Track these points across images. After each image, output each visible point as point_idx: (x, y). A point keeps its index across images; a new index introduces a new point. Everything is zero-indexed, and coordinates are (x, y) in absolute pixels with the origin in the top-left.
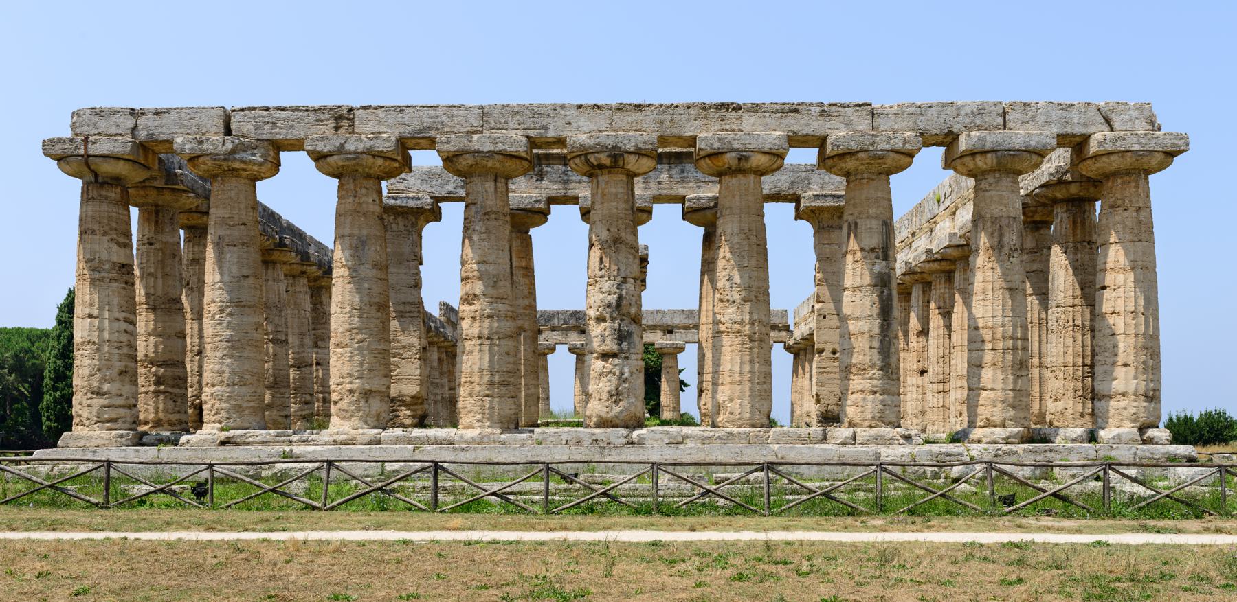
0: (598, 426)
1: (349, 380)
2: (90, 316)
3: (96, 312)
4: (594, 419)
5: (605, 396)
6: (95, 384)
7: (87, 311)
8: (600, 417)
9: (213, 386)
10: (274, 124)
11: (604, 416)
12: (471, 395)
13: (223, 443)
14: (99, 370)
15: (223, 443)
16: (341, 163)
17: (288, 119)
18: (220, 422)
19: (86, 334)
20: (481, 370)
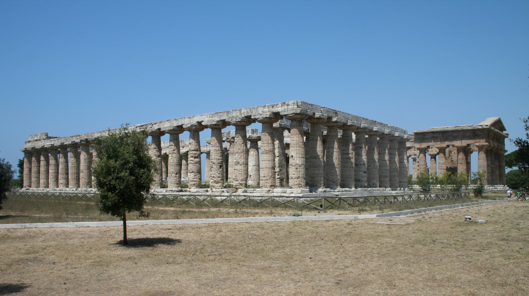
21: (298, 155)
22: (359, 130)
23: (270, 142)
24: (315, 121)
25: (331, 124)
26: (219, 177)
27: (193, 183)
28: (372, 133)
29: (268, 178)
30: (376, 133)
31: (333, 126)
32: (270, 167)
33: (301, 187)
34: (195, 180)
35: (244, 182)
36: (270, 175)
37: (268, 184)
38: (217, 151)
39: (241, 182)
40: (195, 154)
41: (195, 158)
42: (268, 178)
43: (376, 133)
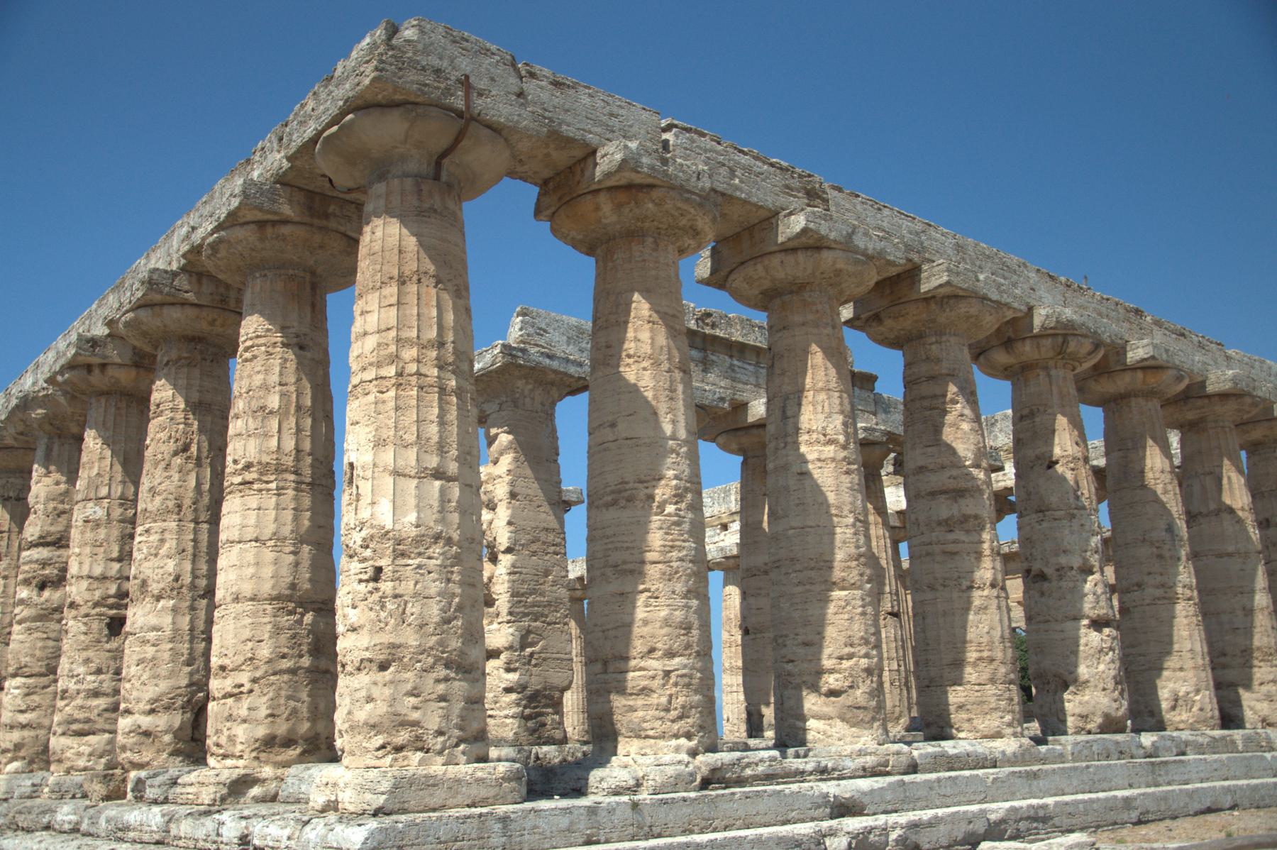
0: (1103, 729)
1: (863, 650)
2: (438, 474)
3: (453, 468)
4: (1099, 720)
5: (1111, 685)
6: (455, 643)
7: (433, 461)
8: (1106, 716)
9: (670, 654)
10: (732, 172)
11: (1114, 714)
12: (992, 681)
13: (706, 784)
14: (460, 608)
15: (706, 784)
16: (840, 265)
17: (747, 169)
18: (689, 736)
19: (431, 517)
20: (1002, 637)
21: (387, 457)
22: (1027, 350)
23: (274, 401)
24: (607, 213)
25: (783, 270)
26: (96, 694)
27: (16, 736)
28: (1123, 383)
29: (244, 678)
30: (1152, 380)
31: (798, 288)
32: (267, 588)
33: (419, 744)
34: (23, 718)
35: (177, 719)
36: (265, 652)
37: (241, 731)
38: (97, 524)
39: (146, 722)
40: (44, 564)
41: (42, 587)
42: (244, 678)
43: (1152, 380)
